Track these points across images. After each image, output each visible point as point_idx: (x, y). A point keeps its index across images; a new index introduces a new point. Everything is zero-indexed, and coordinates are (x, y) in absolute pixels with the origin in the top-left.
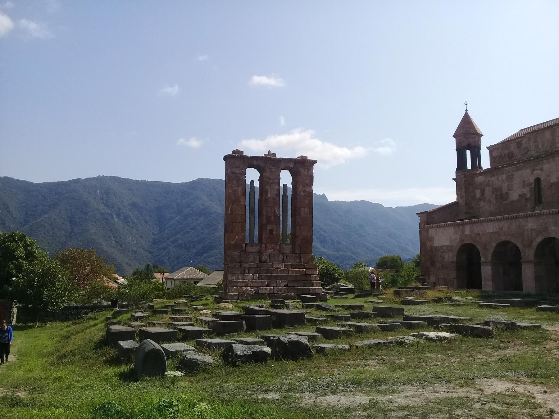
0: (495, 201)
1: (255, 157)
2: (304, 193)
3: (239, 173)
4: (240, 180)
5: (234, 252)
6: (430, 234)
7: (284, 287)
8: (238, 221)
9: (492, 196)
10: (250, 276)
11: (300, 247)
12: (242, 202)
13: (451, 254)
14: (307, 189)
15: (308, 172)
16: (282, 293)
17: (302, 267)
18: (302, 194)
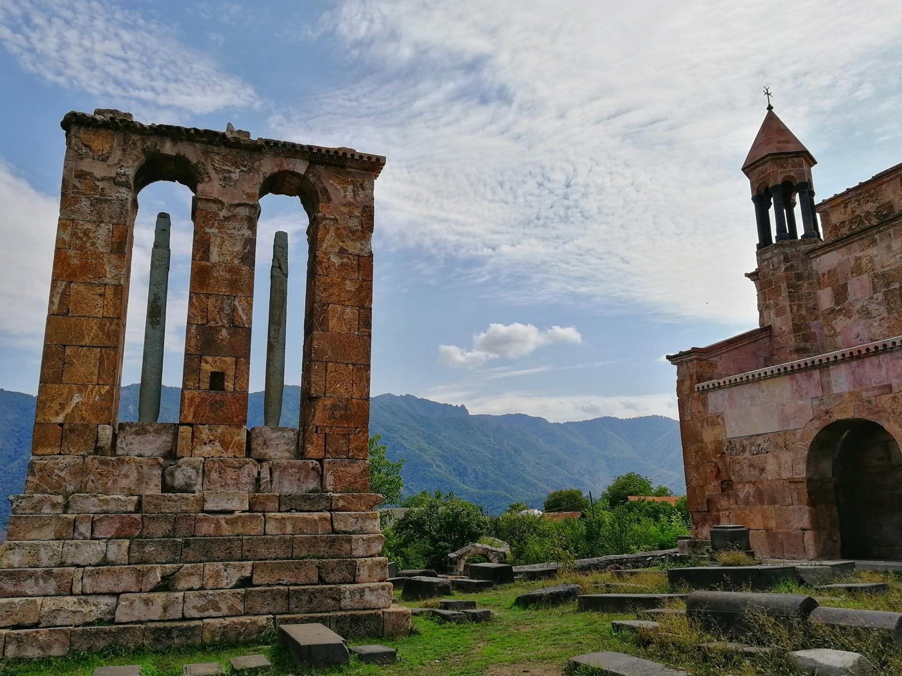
0: (882, 309)
1: (169, 128)
2: (342, 258)
3: (103, 179)
4: (106, 201)
5: (60, 454)
6: (711, 408)
7: (235, 587)
8: (87, 341)
9: (872, 298)
10: (90, 552)
11: (322, 436)
12: (108, 276)
13: (786, 457)
14: (353, 247)
15: (355, 195)
16: (220, 614)
17: (321, 508)
18: (335, 260)
